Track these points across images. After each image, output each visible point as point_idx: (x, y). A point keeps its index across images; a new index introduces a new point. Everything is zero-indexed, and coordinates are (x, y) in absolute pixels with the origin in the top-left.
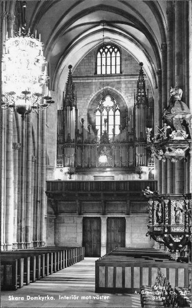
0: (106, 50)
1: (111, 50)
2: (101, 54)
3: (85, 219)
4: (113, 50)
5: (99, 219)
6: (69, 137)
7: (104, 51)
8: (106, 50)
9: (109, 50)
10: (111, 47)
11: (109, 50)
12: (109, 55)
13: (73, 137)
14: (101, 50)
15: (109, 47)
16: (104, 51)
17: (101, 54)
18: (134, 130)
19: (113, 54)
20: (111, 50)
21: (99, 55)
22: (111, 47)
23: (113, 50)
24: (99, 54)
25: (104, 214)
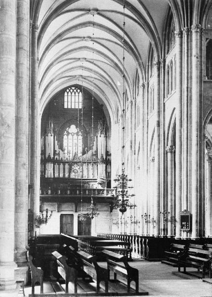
0: (71, 91)
2: (68, 93)
3: (62, 216)
4: (77, 91)
5: (72, 215)
6: (49, 156)
7: (70, 91)
8: (71, 91)
9: (73, 91)
10: (75, 89)
11: (73, 91)
14: (68, 90)
15: (73, 88)
16: (70, 91)
17: (68, 93)
18: (97, 151)
19: (77, 94)
20: (75, 91)
21: (66, 94)
22: (75, 89)
23: (77, 91)
24: (66, 92)
25: (76, 212)
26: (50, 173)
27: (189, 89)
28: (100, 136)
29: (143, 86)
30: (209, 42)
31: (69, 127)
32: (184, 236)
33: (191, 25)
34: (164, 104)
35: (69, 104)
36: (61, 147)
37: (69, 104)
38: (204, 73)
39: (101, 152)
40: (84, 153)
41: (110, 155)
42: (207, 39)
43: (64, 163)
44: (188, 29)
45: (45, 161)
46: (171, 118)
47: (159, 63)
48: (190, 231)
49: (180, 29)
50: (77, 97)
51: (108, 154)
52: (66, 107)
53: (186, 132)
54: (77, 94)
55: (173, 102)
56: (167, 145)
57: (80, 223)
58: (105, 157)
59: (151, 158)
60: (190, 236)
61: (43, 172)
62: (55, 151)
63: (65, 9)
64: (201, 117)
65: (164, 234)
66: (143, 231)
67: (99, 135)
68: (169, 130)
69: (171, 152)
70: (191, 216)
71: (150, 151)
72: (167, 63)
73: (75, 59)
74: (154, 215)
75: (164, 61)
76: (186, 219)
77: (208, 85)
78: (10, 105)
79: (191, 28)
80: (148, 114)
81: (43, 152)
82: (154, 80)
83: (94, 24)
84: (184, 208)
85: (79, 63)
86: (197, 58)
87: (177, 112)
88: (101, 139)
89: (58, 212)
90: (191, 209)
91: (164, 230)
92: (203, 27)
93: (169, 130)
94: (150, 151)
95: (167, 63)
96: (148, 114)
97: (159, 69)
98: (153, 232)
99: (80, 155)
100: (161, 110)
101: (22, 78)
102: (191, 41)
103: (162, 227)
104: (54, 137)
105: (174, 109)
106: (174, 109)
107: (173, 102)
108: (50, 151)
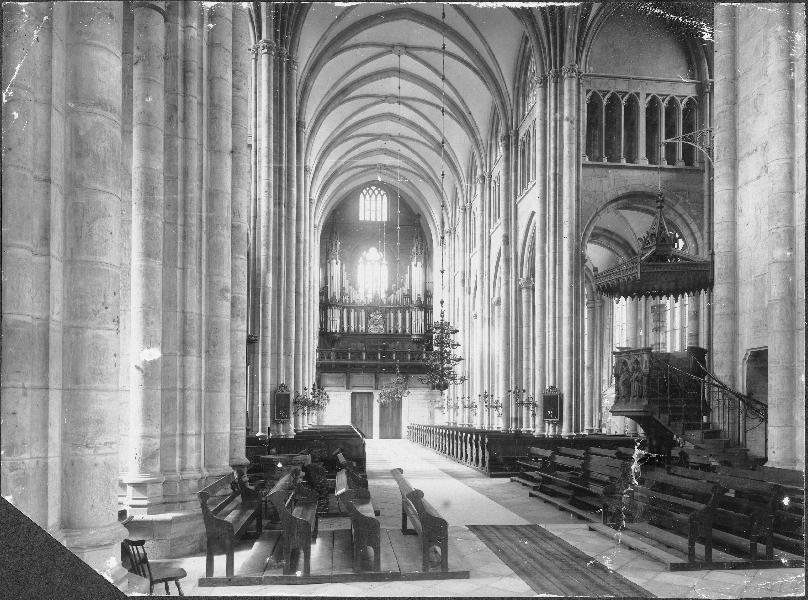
0: (370, 192)
1: (376, 192)
2: (365, 196)
3: (354, 395)
4: (379, 192)
8: (370, 192)
9: (374, 192)
11: (374, 192)
12: (374, 196)
13: (338, 297)
14: (365, 191)
15: (373, 188)
17: (365, 196)
18: (410, 291)
19: (379, 196)
20: (376, 192)
23: (379, 192)
25: (376, 389)
26: (335, 327)
27: (558, 178)
28: (416, 265)
29: (483, 178)
30: (592, 97)
31: (367, 252)
32: (549, 431)
33: (562, 64)
34: (516, 206)
35: (367, 213)
36: (353, 284)
37: (367, 213)
38: (582, 152)
39: (418, 291)
40: (389, 293)
41: (431, 297)
42: (588, 92)
43: (358, 308)
44: (556, 72)
45: (325, 306)
46: (527, 230)
47: (507, 137)
48: (560, 422)
49: (543, 72)
50: (373, 203)
51: (428, 294)
52: (361, 218)
53: (552, 251)
54: (379, 196)
55: (530, 203)
56: (521, 276)
57: (383, 407)
58: (422, 300)
59: (495, 299)
60: (560, 431)
61: (324, 323)
62: (343, 289)
63: (348, 43)
64: (578, 226)
65: (516, 427)
66: (482, 420)
67: (413, 263)
68: (524, 249)
69: (528, 288)
70: (562, 396)
71: (494, 287)
72: (521, 135)
73: (372, 135)
74: (500, 395)
75: (517, 133)
76: (552, 404)
77: (590, 171)
78: (102, 104)
79: (561, 71)
80: (490, 224)
81: (324, 292)
82: (499, 169)
83: (399, 72)
84: (550, 383)
85: (379, 144)
86: (572, 122)
87: (537, 218)
88: (416, 271)
89: (348, 388)
90: (561, 384)
91: (516, 419)
92: (582, 69)
93: (524, 249)
94: (494, 287)
95: (520, 138)
96: (490, 224)
97: (507, 148)
98: (499, 424)
99: (383, 296)
100: (511, 219)
101: (221, 107)
102: (562, 93)
103: (513, 415)
104: (342, 264)
105: (533, 213)
106: (533, 213)
107: (530, 203)
108: (335, 289)
